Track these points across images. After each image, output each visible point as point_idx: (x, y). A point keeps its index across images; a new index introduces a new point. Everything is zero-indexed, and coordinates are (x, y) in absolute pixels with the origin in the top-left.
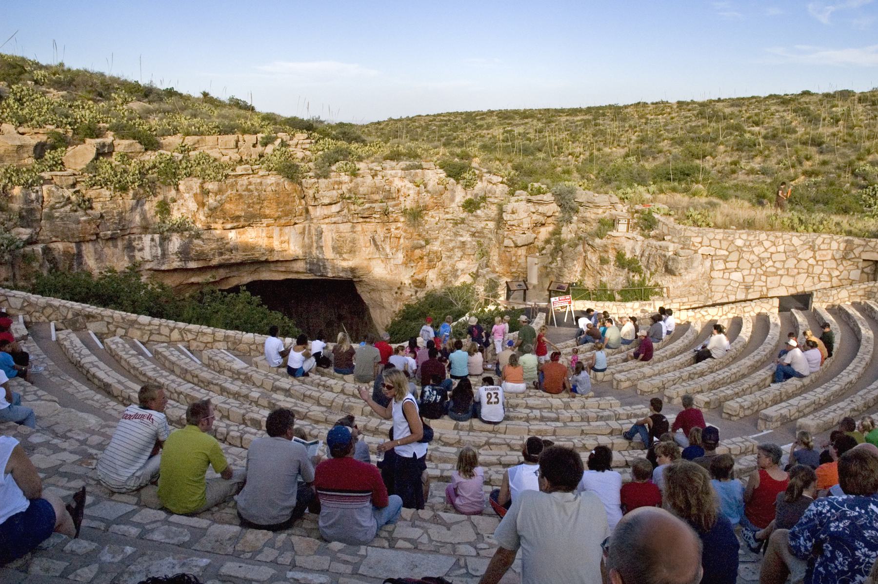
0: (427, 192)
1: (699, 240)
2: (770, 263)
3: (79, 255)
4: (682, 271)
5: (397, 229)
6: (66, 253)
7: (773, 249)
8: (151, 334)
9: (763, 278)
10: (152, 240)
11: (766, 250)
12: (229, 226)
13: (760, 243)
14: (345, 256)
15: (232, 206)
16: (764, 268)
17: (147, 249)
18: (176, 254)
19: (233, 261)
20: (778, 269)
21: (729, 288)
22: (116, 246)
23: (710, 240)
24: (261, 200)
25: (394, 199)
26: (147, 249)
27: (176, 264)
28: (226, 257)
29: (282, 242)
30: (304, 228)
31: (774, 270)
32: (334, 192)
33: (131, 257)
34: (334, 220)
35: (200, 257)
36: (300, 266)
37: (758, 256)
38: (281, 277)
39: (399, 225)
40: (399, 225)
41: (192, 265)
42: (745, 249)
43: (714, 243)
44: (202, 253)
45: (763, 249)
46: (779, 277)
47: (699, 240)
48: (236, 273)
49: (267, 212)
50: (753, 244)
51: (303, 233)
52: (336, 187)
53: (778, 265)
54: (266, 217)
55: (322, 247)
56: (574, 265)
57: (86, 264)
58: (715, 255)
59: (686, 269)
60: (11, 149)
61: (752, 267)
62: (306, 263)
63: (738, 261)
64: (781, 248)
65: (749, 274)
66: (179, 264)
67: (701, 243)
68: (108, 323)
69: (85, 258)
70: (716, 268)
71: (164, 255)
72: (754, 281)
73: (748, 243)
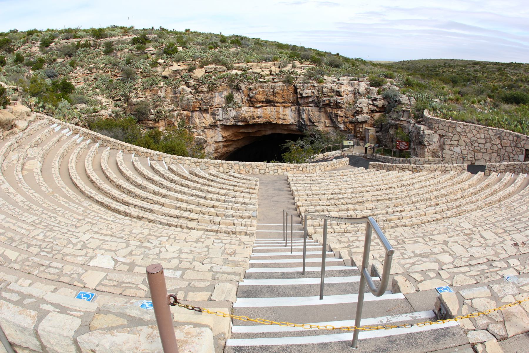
1: (437, 125)
2: (476, 144)
3: (192, 117)
4: (425, 143)
6: (187, 116)
7: (478, 136)
9: (473, 153)
11: (474, 136)
13: (471, 131)
14: (315, 124)
15: (260, 96)
16: (473, 147)
20: (481, 148)
21: (453, 156)
24: (274, 94)
25: (341, 96)
26: (221, 115)
27: (232, 123)
31: (479, 148)
32: (310, 91)
33: (214, 119)
35: (244, 120)
36: (294, 127)
37: (470, 139)
38: (286, 133)
39: (343, 110)
43: (445, 128)
44: (245, 118)
45: (472, 135)
46: (481, 154)
47: (437, 125)
48: (263, 129)
49: (277, 99)
50: (467, 132)
53: (481, 146)
58: (446, 135)
59: (428, 142)
61: (466, 145)
63: (458, 141)
64: (483, 136)
65: (465, 149)
67: (438, 127)
72: (467, 154)
73: (464, 130)
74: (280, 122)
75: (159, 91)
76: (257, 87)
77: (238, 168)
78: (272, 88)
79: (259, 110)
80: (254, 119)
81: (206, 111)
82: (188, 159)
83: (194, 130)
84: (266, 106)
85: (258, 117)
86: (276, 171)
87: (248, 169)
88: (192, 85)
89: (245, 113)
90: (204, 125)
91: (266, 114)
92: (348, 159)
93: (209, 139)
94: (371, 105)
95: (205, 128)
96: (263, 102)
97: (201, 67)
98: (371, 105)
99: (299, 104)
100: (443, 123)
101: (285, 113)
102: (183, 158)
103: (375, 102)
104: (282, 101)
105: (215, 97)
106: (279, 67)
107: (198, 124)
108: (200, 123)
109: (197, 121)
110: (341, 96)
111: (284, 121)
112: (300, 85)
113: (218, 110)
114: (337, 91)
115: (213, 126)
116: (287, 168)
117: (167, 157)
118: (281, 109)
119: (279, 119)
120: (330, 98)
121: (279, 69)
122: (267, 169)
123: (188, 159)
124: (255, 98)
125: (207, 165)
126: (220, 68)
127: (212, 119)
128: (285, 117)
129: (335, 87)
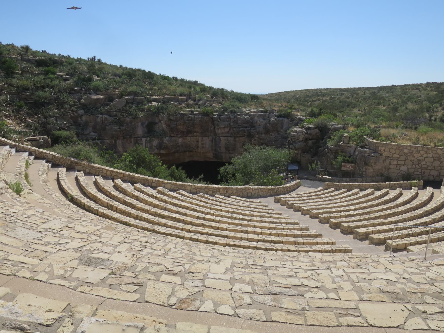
0: (270, 124)
1: (384, 148)
2: (424, 163)
5: (255, 140)
7: (425, 155)
8: (99, 172)
9: (420, 170)
10: (146, 140)
12: (179, 136)
14: (231, 152)
15: (181, 127)
16: (420, 165)
18: (156, 147)
20: (428, 166)
23: (389, 149)
29: (202, 144)
30: (213, 138)
31: (426, 166)
32: (227, 122)
34: (226, 135)
35: (166, 148)
36: (210, 155)
37: (417, 158)
39: (256, 138)
40: (256, 138)
41: (163, 152)
42: (409, 155)
46: (429, 171)
47: (383, 148)
49: (196, 130)
51: (212, 140)
52: (228, 120)
53: (428, 164)
54: (196, 132)
55: (220, 147)
56: (323, 159)
58: (392, 157)
59: (375, 163)
61: (413, 164)
62: (213, 154)
63: (405, 161)
64: (431, 155)
65: (412, 168)
67: (384, 150)
68: (83, 167)
70: (392, 163)
72: (414, 172)
73: (411, 151)
75: (79, 119)
89: (167, 142)
99: (215, 135)
100: (390, 147)
103: (309, 131)
110: (254, 127)
113: (141, 139)
118: (200, 139)
120: (244, 129)
123: (189, 185)
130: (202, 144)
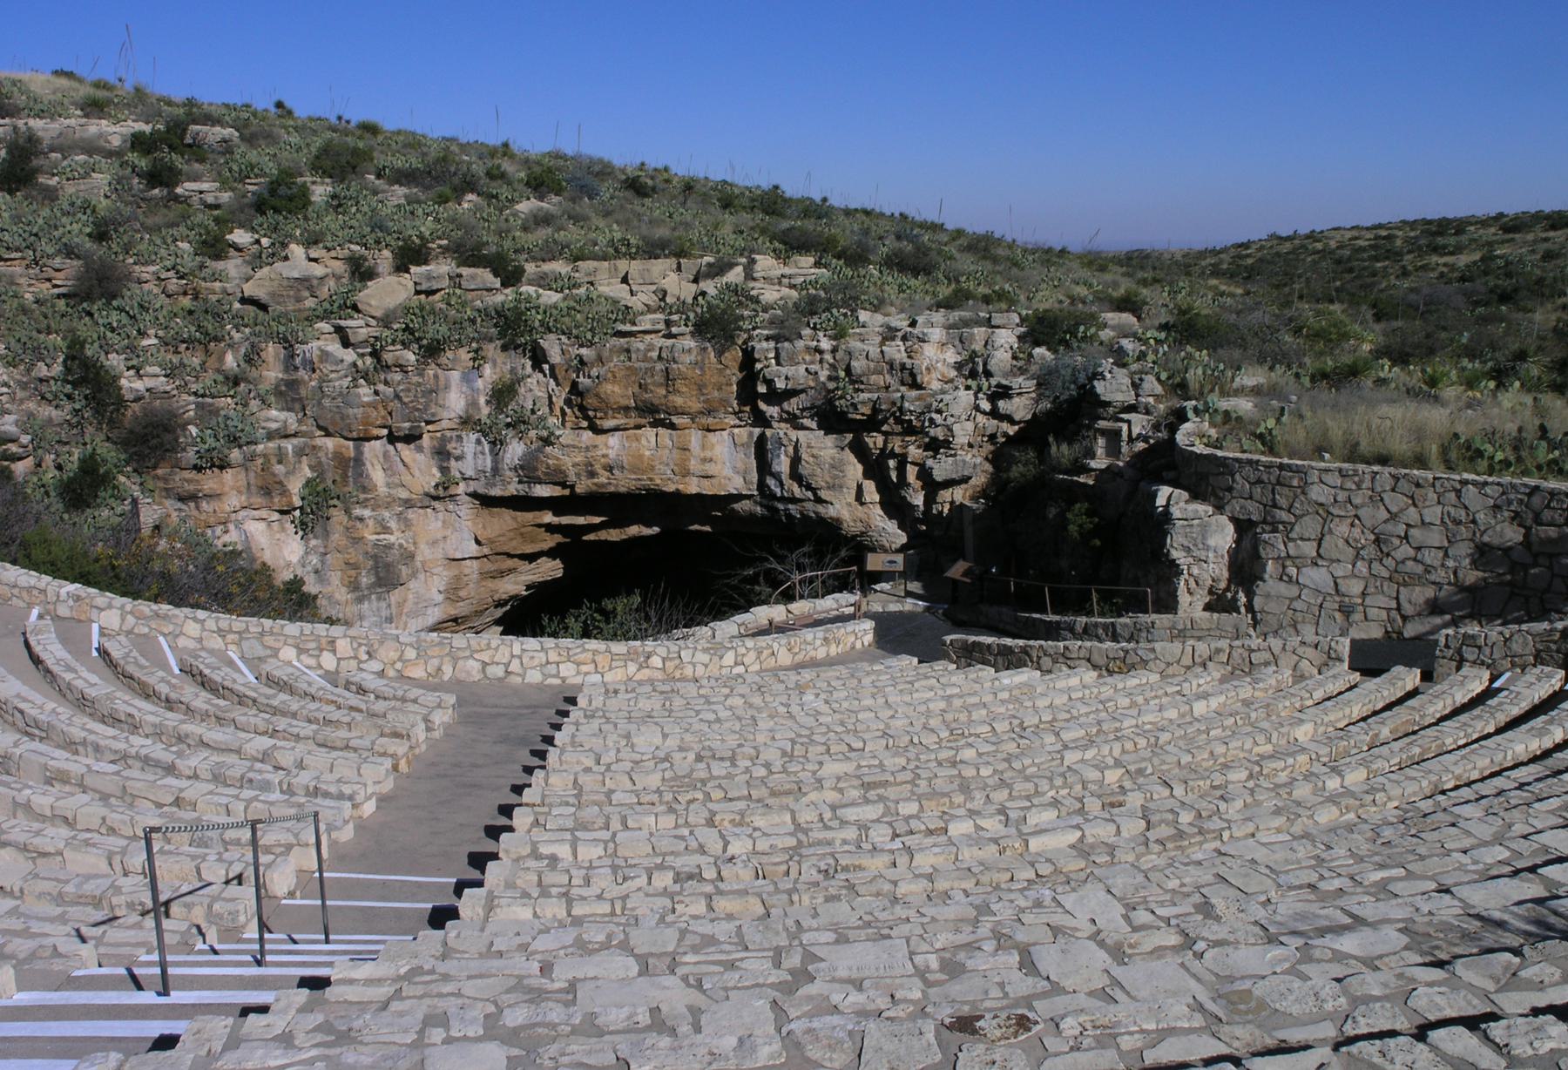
3: (359, 460)
6: (339, 458)
9: (1390, 588)
11: (1393, 517)
13: (1377, 498)
14: (823, 494)
15: (616, 389)
17: (470, 457)
19: (612, 489)
21: (1298, 605)
22: (420, 449)
25: (919, 387)
26: (470, 457)
27: (513, 488)
28: (603, 480)
31: (1419, 569)
33: (444, 470)
41: (542, 491)
42: (1335, 511)
45: (1384, 515)
49: (678, 401)
50: (1357, 501)
52: (808, 358)
53: (1432, 557)
57: (368, 476)
59: (1188, 550)
60: (285, 283)
64: (1433, 514)
66: (520, 487)
69: (369, 466)
71: (496, 470)
73: (1342, 496)
74: (693, 487)
76: (606, 354)
77: (394, 655)
78: (660, 358)
79: (614, 440)
80: (592, 474)
81: (412, 438)
82: (195, 619)
83: (367, 513)
84: (638, 427)
85: (610, 469)
86: (552, 669)
87: (436, 662)
88: (361, 338)
90: (404, 494)
91: (641, 456)
92: (869, 625)
93: (422, 546)
94: (984, 413)
95: (408, 504)
96: (627, 409)
97: (401, 268)
98: (984, 413)
99: (761, 420)
101: (708, 454)
102: (177, 611)
104: (696, 406)
105: (447, 387)
106: (696, 281)
107: (382, 490)
108: (388, 485)
109: (377, 476)
110: (919, 387)
111: (706, 482)
112: (765, 344)
114: (903, 367)
115: (441, 495)
116: (599, 658)
117: (110, 607)
118: (694, 438)
119: (686, 473)
121: (693, 287)
122: (516, 662)
124: (597, 395)
125: (269, 641)
126: (473, 277)
127: (435, 471)
128: (711, 469)
129: (896, 351)
130: (704, 460)
